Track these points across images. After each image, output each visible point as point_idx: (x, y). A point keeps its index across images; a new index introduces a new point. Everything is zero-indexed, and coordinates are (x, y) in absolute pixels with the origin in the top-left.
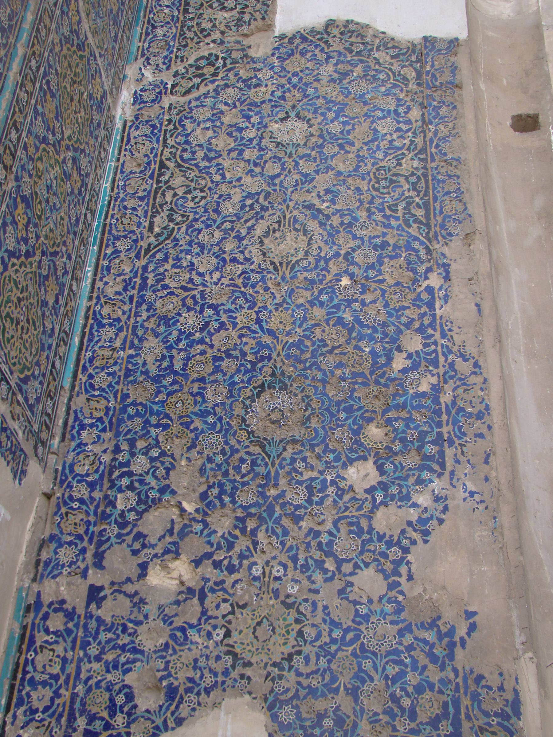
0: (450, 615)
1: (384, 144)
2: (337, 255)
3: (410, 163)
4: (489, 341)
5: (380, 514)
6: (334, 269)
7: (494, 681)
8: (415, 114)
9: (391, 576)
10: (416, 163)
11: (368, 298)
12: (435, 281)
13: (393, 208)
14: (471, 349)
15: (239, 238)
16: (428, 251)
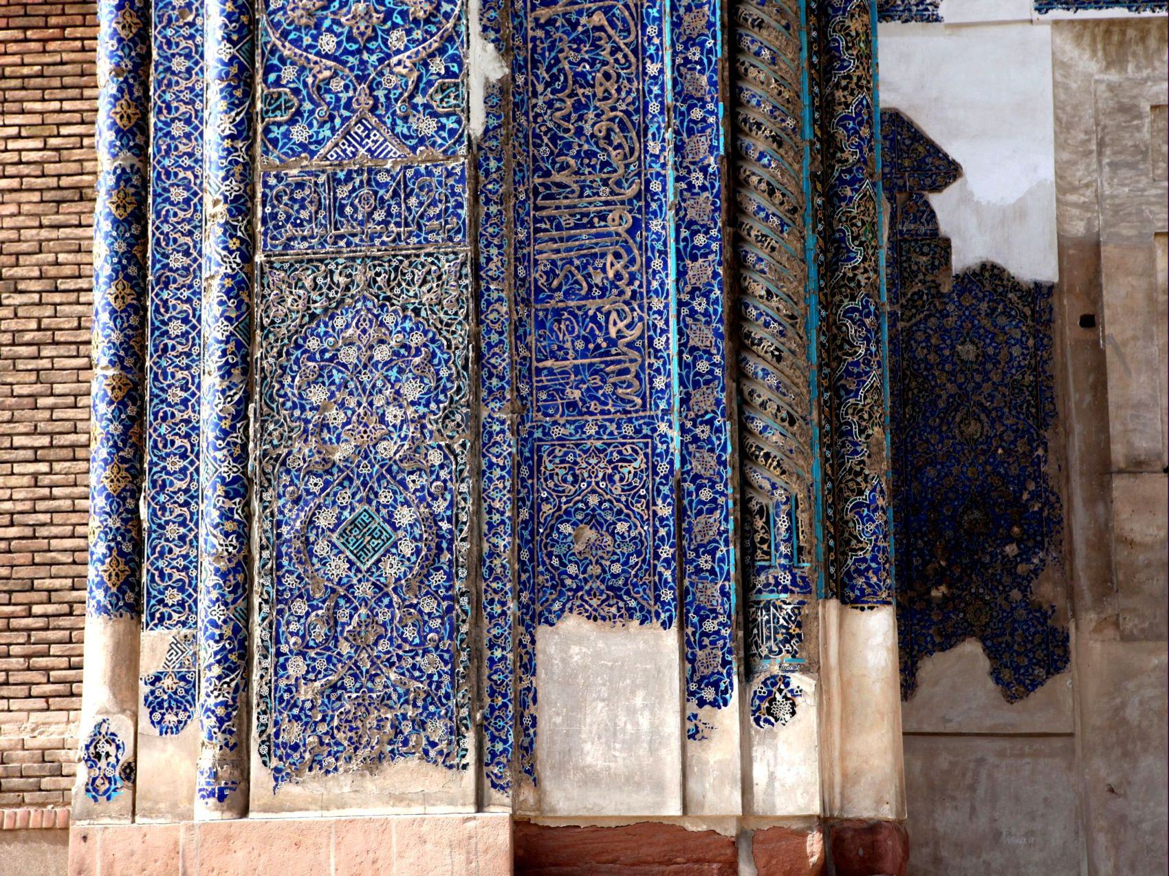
0: (1045, 606)
1: (1016, 364)
2: (995, 435)
3: (1029, 378)
4: (1063, 482)
5: (1019, 567)
6: (995, 444)
7: (1060, 630)
8: (1031, 342)
9: (1023, 592)
10: (1031, 378)
11: (1011, 460)
12: (1040, 452)
13: (1021, 406)
14: (1056, 490)
15: (949, 424)
16: (1038, 435)
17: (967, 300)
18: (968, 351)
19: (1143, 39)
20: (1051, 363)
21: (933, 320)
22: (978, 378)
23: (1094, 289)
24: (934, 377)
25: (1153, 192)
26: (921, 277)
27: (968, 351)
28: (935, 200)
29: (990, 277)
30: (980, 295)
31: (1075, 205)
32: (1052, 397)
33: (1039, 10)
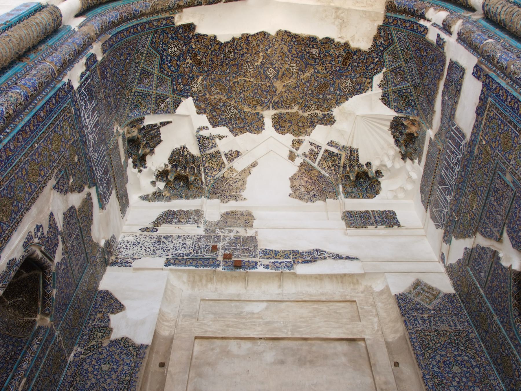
1: (124, 372)
3: (128, 378)
8: (133, 365)
10: (129, 378)
17: (112, 349)
18: (106, 367)
19: (201, 280)
20: (139, 373)
21: (96, 355)
22: (106, 377)
23: (168, 352)
24: (88, 376)
25: (197, 324)
26: (96, 340)
27: (106, 367)
28: (113, 318)
29: (125, 343)
30: (118, 347)
31: (167, 326)
32: (135, 385)
33: (165, 266)
